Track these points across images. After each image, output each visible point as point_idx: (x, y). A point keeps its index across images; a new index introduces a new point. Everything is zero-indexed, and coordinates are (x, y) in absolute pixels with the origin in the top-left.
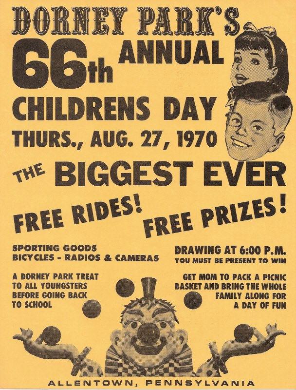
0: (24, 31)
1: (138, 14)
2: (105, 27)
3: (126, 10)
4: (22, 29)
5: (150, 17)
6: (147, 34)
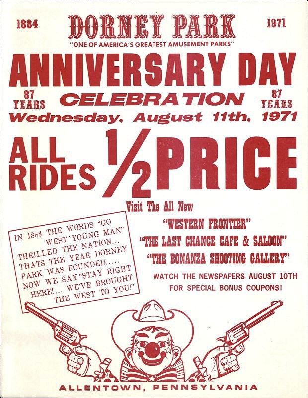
0: (78, 35)
1: (174, 20)
2: (145, 32)
3: (164, 17)
4: (77, 33)
5: (183, 21)
6: (181, 37)
